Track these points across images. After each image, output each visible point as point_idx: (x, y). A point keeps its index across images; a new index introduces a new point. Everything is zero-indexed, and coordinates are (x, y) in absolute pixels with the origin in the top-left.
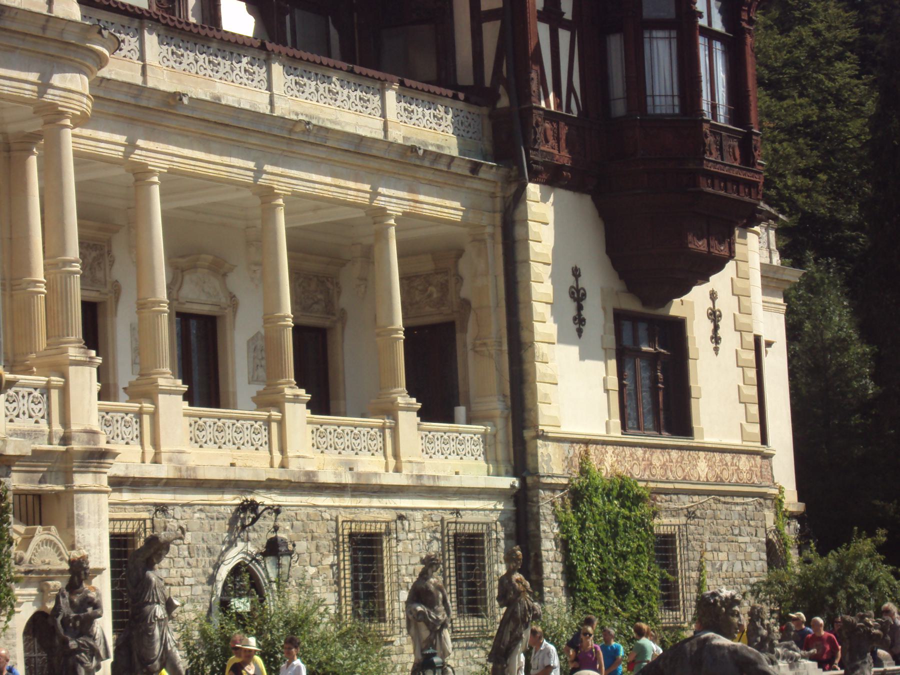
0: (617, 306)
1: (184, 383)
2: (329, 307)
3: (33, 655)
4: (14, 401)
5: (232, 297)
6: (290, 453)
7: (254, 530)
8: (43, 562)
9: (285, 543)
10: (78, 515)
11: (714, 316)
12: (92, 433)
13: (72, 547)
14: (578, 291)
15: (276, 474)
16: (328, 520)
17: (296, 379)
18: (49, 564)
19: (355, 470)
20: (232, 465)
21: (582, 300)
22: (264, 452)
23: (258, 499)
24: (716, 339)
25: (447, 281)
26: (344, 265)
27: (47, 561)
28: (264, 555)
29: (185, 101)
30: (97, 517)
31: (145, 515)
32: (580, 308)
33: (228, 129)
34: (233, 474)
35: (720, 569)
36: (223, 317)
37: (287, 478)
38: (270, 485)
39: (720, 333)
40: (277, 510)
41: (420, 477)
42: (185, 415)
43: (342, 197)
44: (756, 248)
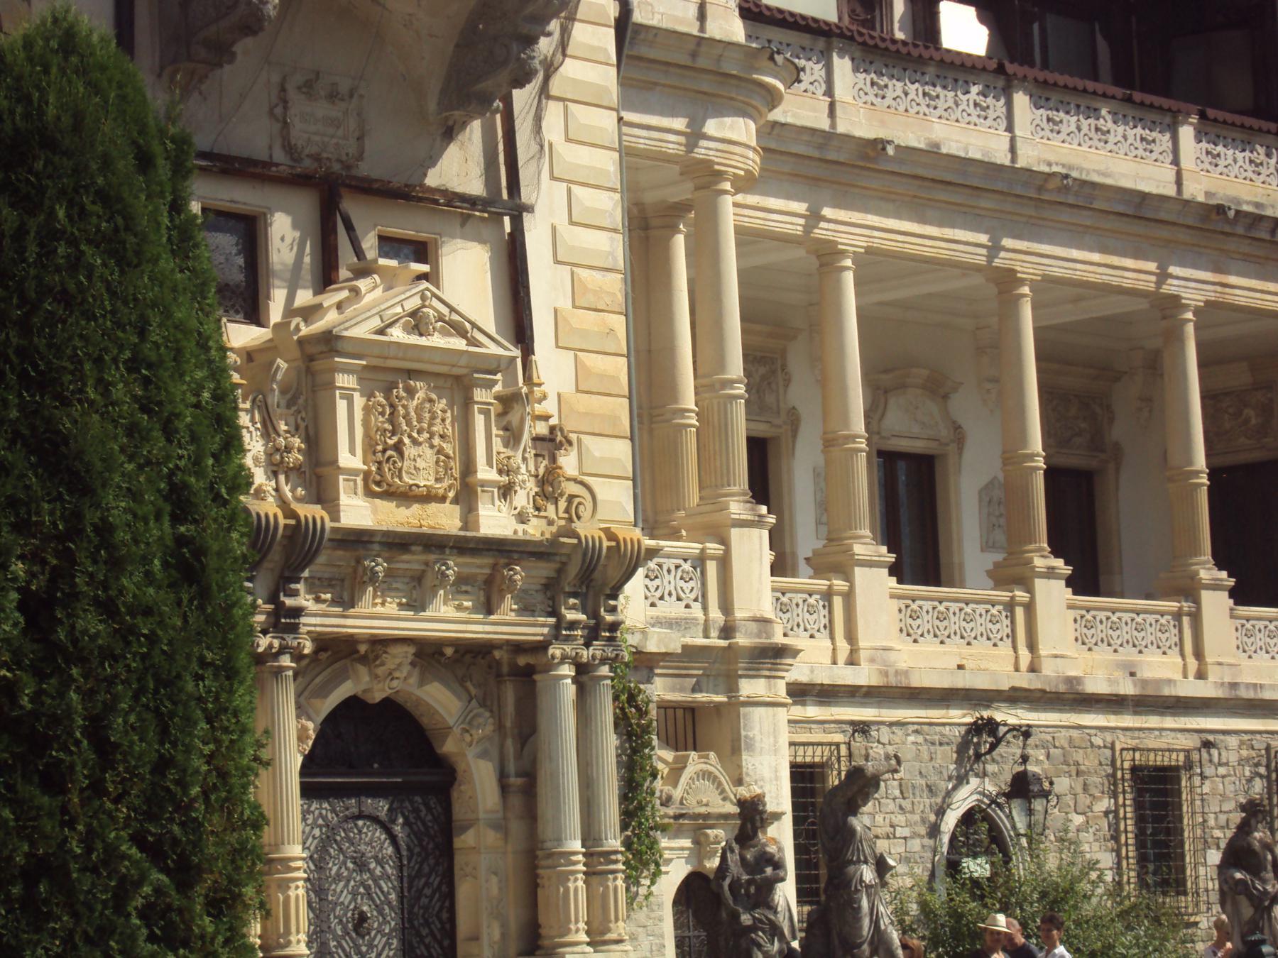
2: (1097, 443)
3: (686, 934)
5: (957, 428)
6: (1044, 650)
7: (993, 760)
8: (700, 803)
9: (1038, 779)
10: (746, 737)
12: (764, 621)
13: (739, 782)
15: (1024, 680)
16: (1099, 747)
18: (707, 805)
19: (1139, 675)
20: (960, 667)
22: (1005, 649)
23: (999, 717)
27: (705, 801)
28: (1009, 796)
29: (890, 151)
30: (772, 740)
31: (838, 738)
33: (950, 188)
34: (961, 681)
37: (1039, 687)
38: (1015, 697)
40: (1025, 733)
41: (1234, 686)
42: (892, 596)
43: (1115, 281)
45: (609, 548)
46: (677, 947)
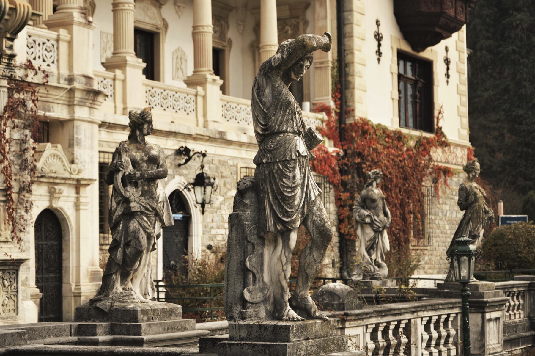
0: (399, 48)
1: (144, 61)
3: (40, 243)
4: (32, 47)
6: (210, 118)
7: (186, 168)
8: (51, 171)
9: (209, 178)
10: (77, 138)
11: (447, 62)
13: (72, 162)
14: (378, 34)
15: (201, 131)
16: (231, 166)
17: (213, 69)
18: (55, 173)
19: (248, 134)
20: (172, 122)
21: (381, 40)
22: (193, 115)
24: (448, 76)
25: (298, 23)
26: (231, 10)
27: (54, 171)
32: (379, 45)
35: (446, 215)
36: (158, 34)
37: (208, 134)
39: (450, 72)
42: (143, 84)
44: (464, 27)
45: (10, 8)
46: (36, 249)
